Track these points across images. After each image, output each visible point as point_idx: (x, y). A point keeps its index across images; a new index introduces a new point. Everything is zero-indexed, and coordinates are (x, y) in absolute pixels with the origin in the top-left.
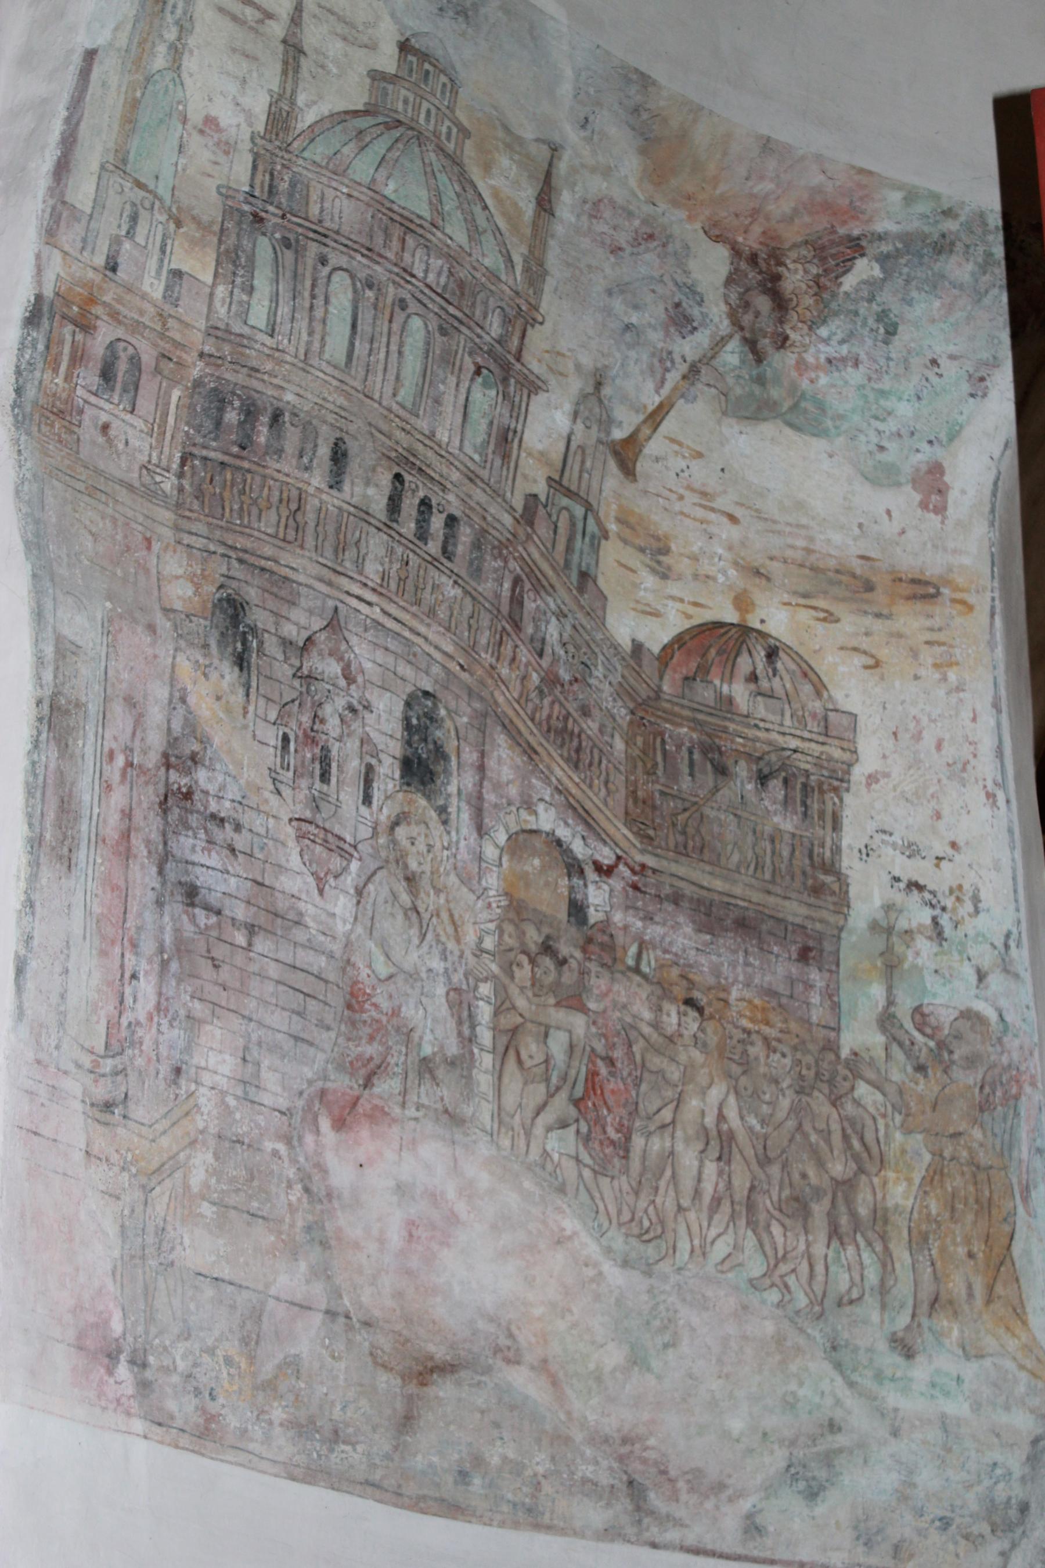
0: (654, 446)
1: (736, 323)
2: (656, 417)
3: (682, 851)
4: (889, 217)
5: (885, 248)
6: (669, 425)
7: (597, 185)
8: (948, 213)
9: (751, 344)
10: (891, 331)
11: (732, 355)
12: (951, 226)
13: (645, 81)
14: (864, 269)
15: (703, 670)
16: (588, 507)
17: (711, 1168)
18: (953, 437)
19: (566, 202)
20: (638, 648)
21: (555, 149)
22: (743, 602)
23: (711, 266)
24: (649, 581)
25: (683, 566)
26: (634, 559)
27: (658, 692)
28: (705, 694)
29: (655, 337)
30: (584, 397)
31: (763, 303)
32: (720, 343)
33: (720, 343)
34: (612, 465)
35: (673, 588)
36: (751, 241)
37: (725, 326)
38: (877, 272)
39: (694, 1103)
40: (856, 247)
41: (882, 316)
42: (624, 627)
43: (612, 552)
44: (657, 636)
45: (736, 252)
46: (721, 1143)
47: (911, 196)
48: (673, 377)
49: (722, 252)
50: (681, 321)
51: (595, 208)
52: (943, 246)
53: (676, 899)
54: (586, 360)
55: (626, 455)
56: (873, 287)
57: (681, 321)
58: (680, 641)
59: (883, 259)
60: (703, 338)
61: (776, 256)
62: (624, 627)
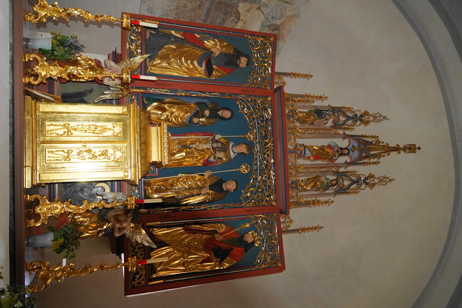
0: (260, 12)
1: (272, 24)
2: (263, 13)
3: (216, 7)
6: (262, 14)
7: (288, 9)
9: (269, 26)
11: (269, 23)
13: (298, 17)
15: (235, 14)
16: (254, 3)
17: (182, 5)
19: (286, 5)
20: (238, 6)
21: (292, 4)
22: (242, 20)
23: (278, 22)
24: (245, 9)
25: (246, 14)
26: (248, 7)
27: (233, 8)
28: (233, 14)
29: (271, 14)
30: (265, 4)
31: (274, 28)
32: (270, 22)
33: (270, 22)
34: (258, 6)
35: (244, 12)
36: (280, 28)
37: (272, 23)
39: (189, 4)
42: (241, 5)
43: (249, 5)
44: (239, 9)
45: (279, 25)
46: (185, 6)
47: (282, 46)
48: (267, 16)
49: (280, 24)
50: (273, 18)
51: (286, 9)
53: (211, 6)
54: (269, 5)
55: (259, 8)
57: (273, 18)
58: (239, 11)
60: (271, 20)
61: (278, 30)
62: (241, 5)
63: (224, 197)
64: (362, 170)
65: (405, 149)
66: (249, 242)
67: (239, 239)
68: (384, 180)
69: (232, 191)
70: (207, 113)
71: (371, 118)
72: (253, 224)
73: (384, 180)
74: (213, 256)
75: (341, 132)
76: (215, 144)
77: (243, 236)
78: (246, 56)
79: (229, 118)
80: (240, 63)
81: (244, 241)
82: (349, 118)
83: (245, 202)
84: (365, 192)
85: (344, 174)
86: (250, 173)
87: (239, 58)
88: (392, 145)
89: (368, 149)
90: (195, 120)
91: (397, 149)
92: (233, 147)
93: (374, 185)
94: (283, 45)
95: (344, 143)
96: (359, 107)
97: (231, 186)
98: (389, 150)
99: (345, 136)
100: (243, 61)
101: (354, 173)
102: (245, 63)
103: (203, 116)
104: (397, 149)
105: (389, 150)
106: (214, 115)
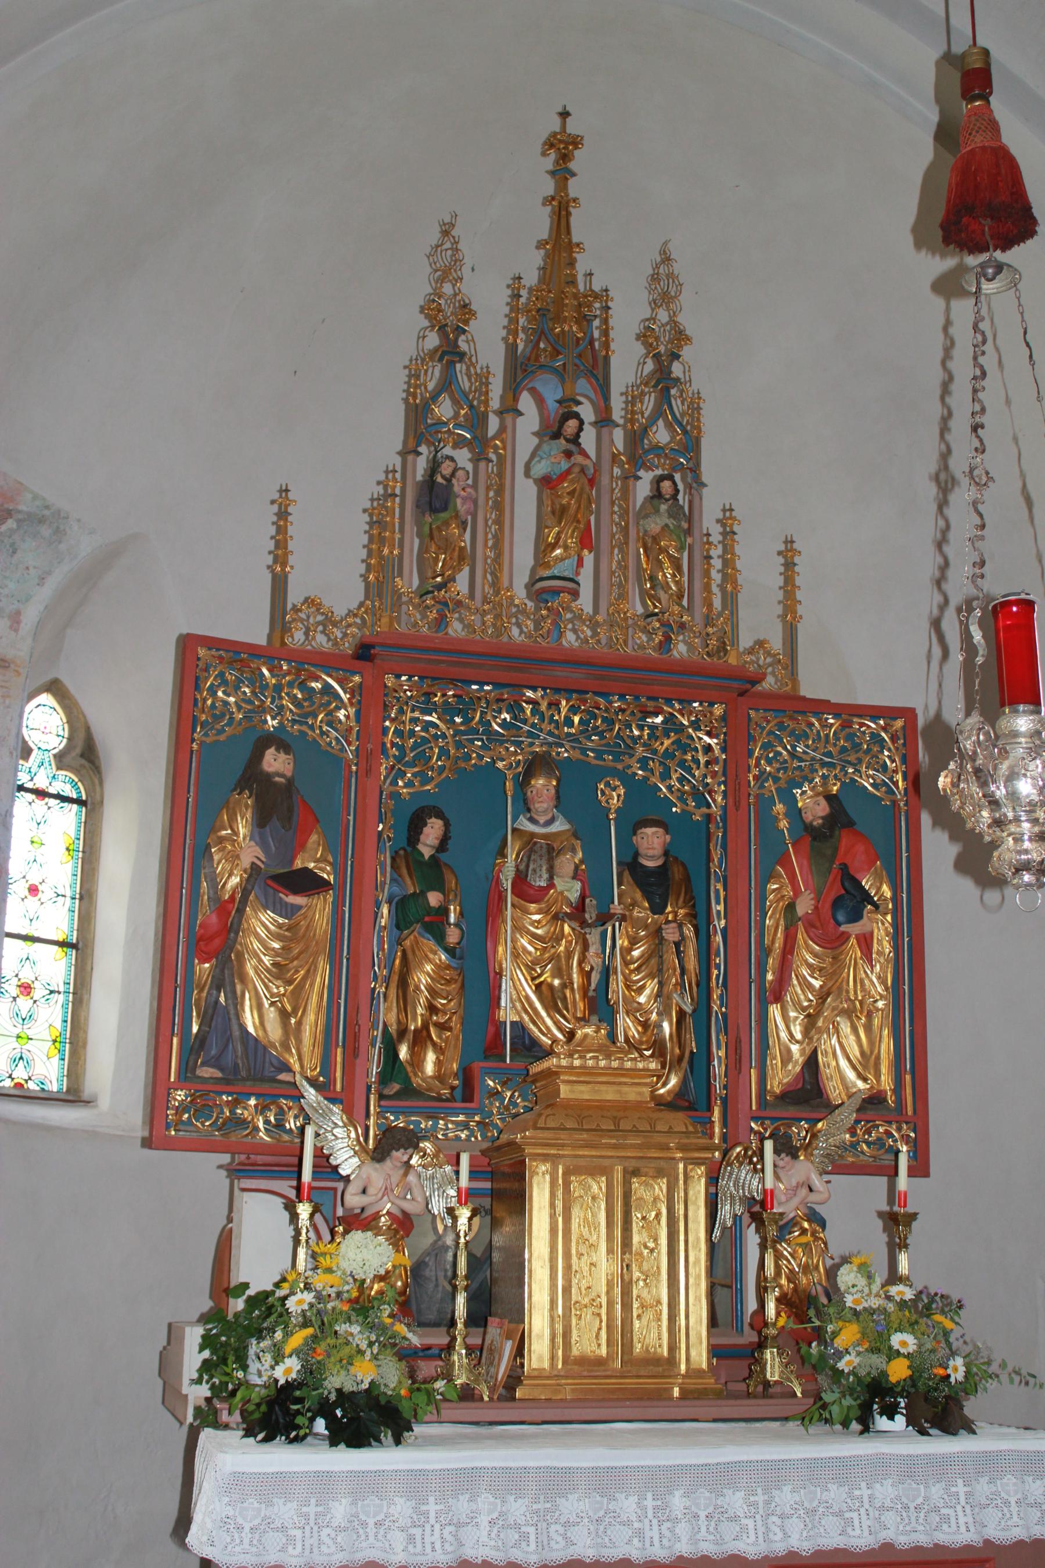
4: (25, 505)
5: (20, 516)
8: (47, 507)
10: (14, 552)
12: (46, 512)
14: (11, 523)
18: (27, 600)
38: (15, 526)
40: (9, 514)
41: (12, 545)
47: (35, 497)
52: (42, 521)
56: (12, 532)
59: (19, 521)
63: (683, 864)
64: (627, 364)
65: (562, 174)
66: (828, 810)
67: (814, 839)
68: (663, 286)
69: (668, 838)
70: (434, 899)
71: (447, 289)
72: (776, 789)
73: (663, 286)
74: (854, 929)
75: (493, 424)
76: (587, 916)
77: (808, 828)
78: (257, 755)
79: (447, 825)
80: (282, 776)
81: (823, 825)
82: (447, 384)
83: (709, 806)
84: (698, 367)
85: (636, 437)
86: (627, 779)
87: (268, 776)
88: (542, 225)
89: (560, 328)
90: (453, 936)
91: (561, 209)
92: (532, 820)
93: (680, 337)
94: (29, 496)
95: (529, 419)
96: (407, 334)
97: (652, 843)
98: (560, 246)
99: (510, 409)
100: (275, 762)
101: (632, 400)
102: (282, 756)
103: (444, 911)
104: (561, 209)
105: (560, 246)
106: (432, 872)
